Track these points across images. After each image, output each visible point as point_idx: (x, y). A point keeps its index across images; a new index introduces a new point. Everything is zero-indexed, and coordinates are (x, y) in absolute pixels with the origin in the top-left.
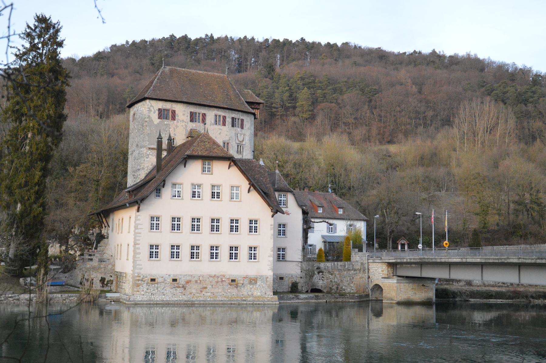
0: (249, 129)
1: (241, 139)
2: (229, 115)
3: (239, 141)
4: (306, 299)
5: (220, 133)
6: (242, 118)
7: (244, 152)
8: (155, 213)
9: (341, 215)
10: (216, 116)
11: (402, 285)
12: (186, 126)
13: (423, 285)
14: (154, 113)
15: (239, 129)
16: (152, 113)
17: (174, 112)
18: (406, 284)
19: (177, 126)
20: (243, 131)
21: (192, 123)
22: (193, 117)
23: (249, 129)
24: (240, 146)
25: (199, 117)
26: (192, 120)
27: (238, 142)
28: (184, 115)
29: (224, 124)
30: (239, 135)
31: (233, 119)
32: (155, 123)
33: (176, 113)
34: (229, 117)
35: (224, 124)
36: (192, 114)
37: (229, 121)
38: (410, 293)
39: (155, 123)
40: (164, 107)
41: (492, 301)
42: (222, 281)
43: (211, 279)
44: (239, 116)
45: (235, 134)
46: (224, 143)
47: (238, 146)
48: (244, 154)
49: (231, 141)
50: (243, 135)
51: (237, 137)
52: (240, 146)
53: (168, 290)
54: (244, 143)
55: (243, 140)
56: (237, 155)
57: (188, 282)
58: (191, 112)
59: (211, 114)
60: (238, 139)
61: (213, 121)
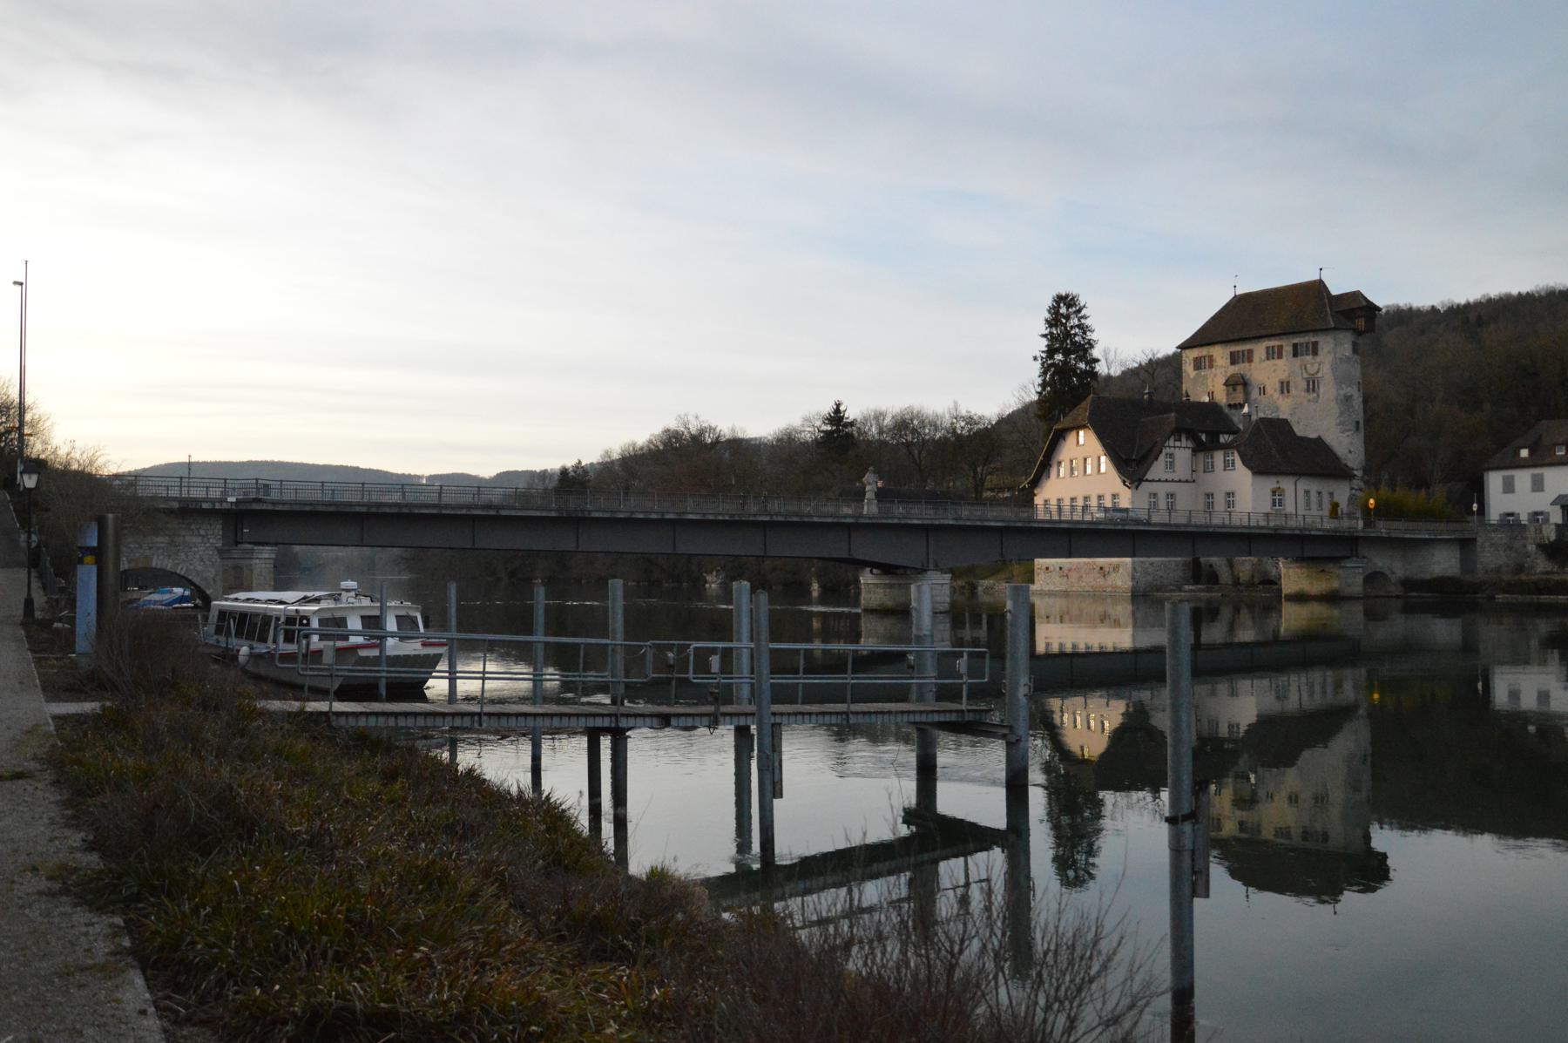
0: (1329, 352)
1: (1312, 369)
2: (1287, 344)
3: (1309, 374)
4: (1191, 591)
5: (1274, 371)
6: (1314, 340)
7: (1321, 386)
8: (1047, 497)
9: (1525, 459)
10: (1268, 348)
11: (1291, 570)
12: (1226, 372)
13: (1323, 571)
14: (1190, 364)
15: (1309, 358)
16: (1188, 365)
17: (1211, 357)
18: (1297, 570)
19: (1215, 375)
20: (1318, 359)
21: (1233, 367)
22: (1234, 359)
23: (1329, 352)
24: (1314, 382)
25: (1243, 356)
26: (1233, 362)
27: (1305, 376)
28: (1222, 358)
29: (1280, 356)
30: (1308, 366)
31: (1295, 346)
32: (1192, 377)
33: (1214, 357)
34: (1288, 345)
35: (1280, 356)
36: (1232, 354)
37: (1288, 349)
38: (1304, 582)
39: (1192, 377)
40: (1200, 355)
41: (1544, 598)
42: (1094, 569)
43: (1086, 567)
44: (1307, 338)
45: (1301, 366)
46: (1282, 383)
47: (1308, 382)
48: (1321, 390)
49: (1292, 378)
50: (1316, 366)
51: (1305, 369)
52: (1314, 382)
53: (1057, 580)
54: (1320, 375)
55: (1318, 372)
56: (1306, 394)
57: (1070, 570)
58: (1231, 353)
59: (1260, 349)
60: (1306, 372)
61: (1264, 356)
